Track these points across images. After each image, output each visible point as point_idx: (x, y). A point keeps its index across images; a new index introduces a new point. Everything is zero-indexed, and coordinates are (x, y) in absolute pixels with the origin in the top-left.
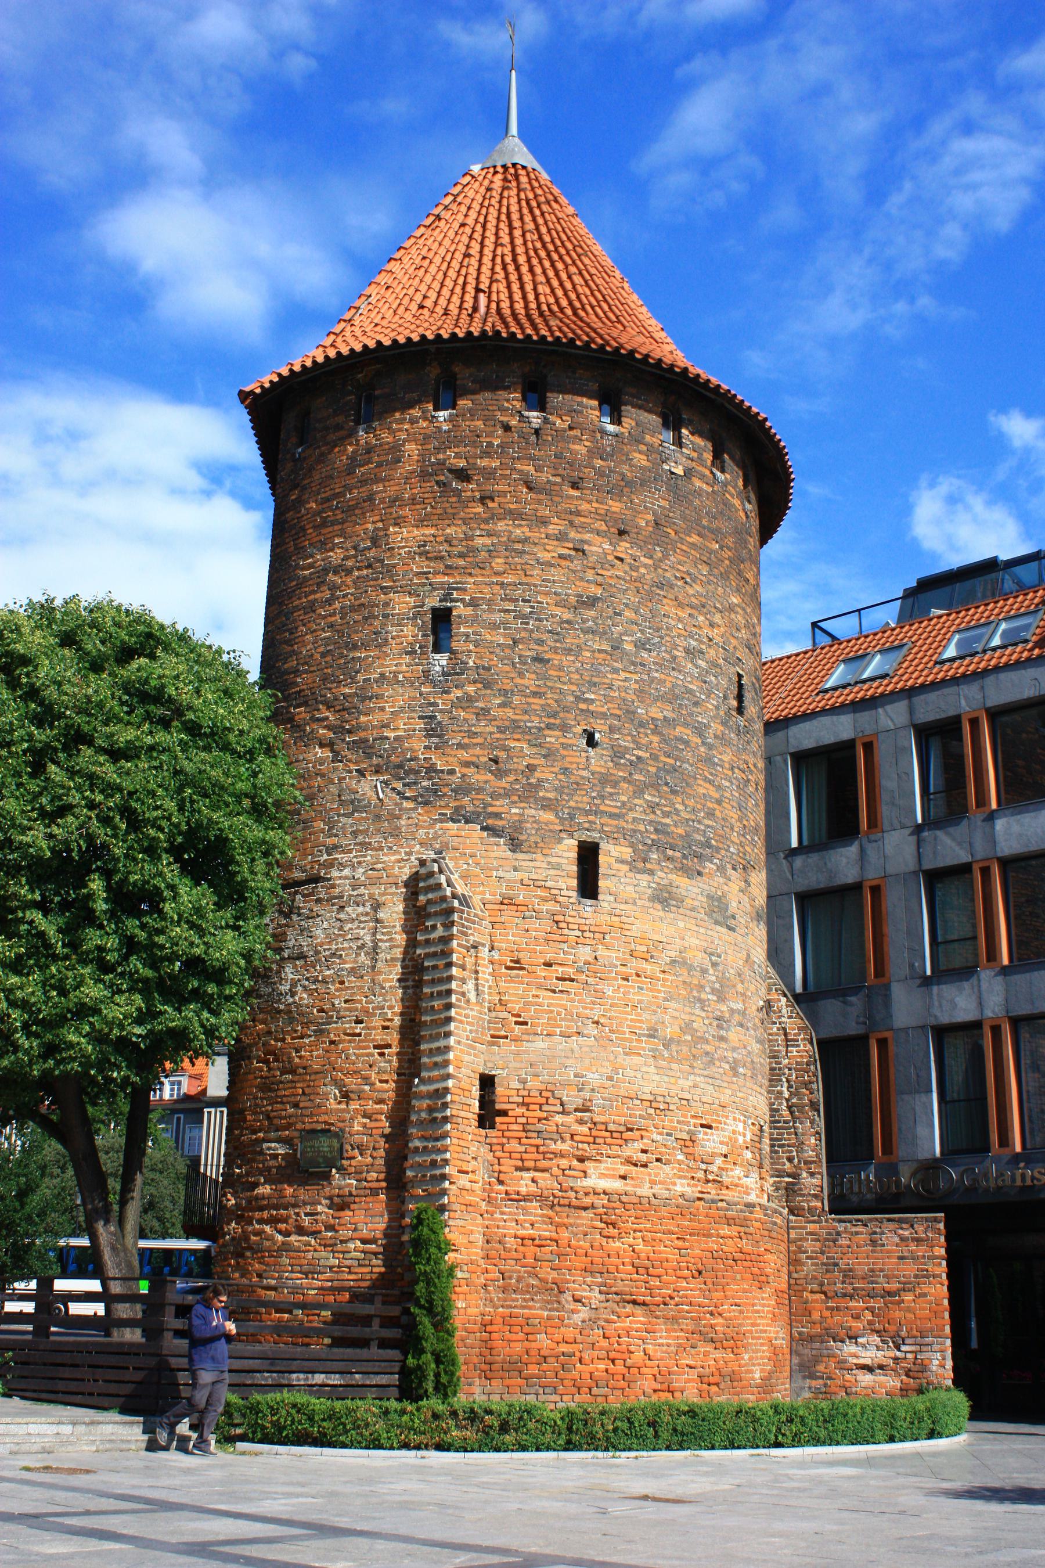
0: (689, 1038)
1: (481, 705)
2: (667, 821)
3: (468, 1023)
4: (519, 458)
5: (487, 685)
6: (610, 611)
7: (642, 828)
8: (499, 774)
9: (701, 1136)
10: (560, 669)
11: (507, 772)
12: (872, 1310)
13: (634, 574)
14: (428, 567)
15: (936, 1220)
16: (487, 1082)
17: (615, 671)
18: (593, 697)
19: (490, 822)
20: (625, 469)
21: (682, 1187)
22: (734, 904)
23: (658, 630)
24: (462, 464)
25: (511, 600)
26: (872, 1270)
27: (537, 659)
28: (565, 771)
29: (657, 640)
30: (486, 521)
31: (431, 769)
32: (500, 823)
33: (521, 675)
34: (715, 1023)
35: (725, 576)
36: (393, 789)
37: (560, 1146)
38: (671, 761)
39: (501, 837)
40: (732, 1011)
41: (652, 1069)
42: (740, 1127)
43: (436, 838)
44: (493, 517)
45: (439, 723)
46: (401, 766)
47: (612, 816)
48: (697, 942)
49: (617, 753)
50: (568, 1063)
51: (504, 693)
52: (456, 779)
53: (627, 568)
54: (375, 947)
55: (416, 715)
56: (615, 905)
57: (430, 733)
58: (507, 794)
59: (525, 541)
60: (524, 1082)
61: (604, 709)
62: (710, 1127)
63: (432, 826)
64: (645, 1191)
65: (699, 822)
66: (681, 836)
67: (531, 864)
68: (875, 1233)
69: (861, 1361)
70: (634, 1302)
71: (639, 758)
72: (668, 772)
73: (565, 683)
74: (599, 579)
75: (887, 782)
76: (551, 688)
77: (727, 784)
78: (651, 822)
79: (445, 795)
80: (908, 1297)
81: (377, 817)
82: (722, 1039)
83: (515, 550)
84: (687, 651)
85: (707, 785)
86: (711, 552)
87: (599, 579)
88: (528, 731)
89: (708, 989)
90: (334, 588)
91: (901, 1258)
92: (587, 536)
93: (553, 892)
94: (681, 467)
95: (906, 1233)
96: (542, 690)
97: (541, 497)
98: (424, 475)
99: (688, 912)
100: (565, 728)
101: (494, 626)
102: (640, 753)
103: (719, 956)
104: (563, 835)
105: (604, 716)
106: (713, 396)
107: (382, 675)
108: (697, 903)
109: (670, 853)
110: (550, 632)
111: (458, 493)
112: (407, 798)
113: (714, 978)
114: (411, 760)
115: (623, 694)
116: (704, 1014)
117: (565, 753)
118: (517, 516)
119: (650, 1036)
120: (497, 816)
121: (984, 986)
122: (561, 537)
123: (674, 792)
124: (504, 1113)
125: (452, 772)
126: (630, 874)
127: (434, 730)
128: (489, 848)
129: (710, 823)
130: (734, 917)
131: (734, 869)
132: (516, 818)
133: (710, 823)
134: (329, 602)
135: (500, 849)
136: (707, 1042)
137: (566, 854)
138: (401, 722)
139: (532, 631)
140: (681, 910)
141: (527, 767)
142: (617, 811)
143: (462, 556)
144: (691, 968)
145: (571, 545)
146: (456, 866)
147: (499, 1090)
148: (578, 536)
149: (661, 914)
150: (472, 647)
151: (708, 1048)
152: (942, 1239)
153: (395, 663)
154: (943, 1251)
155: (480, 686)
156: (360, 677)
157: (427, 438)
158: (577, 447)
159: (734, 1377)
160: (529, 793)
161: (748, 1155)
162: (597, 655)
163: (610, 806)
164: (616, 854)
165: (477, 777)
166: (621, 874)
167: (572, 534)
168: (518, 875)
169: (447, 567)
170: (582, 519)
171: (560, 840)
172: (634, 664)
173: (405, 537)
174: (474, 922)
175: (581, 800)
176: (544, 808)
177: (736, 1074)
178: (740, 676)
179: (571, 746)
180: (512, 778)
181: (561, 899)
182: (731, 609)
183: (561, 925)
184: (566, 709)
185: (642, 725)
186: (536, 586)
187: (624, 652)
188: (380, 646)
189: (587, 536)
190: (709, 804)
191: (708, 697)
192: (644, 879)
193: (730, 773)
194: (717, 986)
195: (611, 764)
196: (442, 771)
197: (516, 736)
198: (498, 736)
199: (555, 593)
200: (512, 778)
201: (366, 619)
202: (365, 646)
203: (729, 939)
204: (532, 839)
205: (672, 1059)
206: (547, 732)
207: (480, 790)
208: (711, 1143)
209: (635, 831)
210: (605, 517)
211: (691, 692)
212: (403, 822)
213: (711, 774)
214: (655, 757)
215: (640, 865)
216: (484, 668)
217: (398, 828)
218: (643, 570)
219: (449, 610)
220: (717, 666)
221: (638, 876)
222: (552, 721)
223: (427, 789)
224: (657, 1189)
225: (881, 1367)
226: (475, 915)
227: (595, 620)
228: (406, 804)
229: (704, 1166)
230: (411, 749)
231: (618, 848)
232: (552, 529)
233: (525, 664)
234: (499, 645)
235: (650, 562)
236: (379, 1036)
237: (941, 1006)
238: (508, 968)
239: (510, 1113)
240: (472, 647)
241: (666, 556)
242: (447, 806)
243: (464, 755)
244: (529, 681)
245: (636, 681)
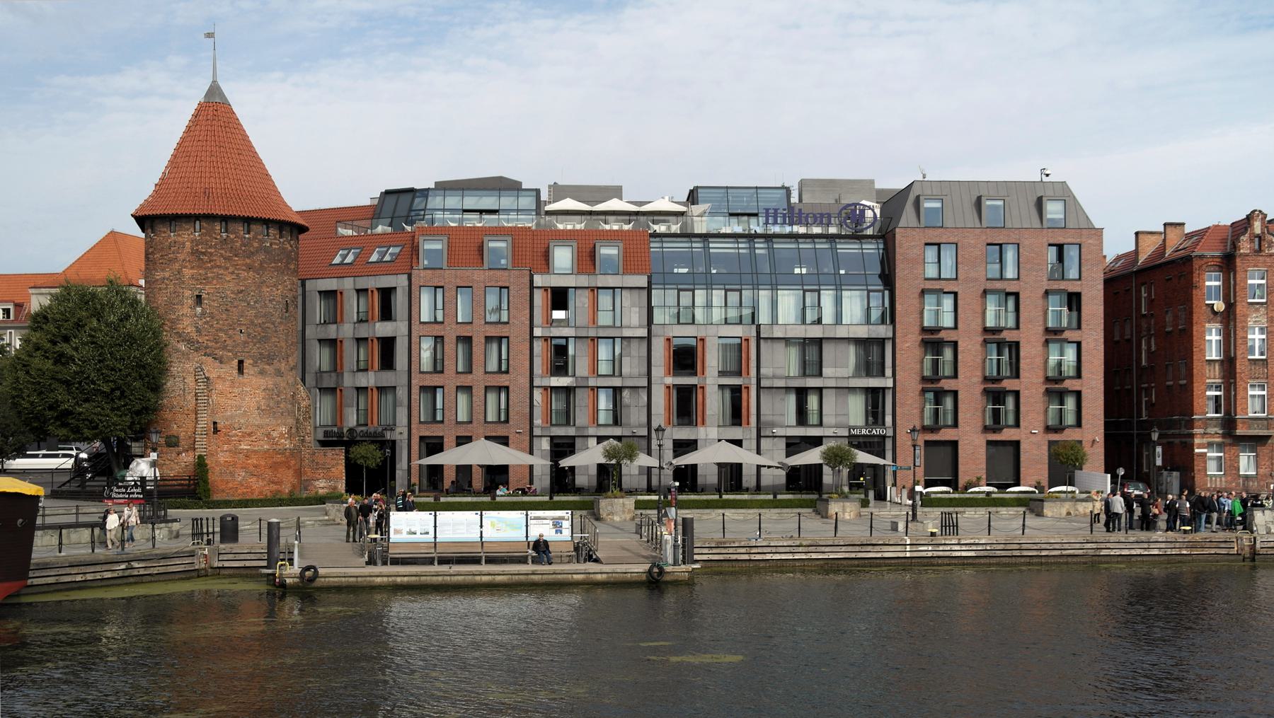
16: (215, 423)
44: (212, 267)
49: (249, 335)
75: (346, 307)
118: (219, 267)
122: (233, 273)
127: (198, 331)
135: (217, 363)
153: (186, 310)
160: (224, 348)
173: (187, 272)
208: (275, 434)
210: (246, 265)
244: (224, 316)
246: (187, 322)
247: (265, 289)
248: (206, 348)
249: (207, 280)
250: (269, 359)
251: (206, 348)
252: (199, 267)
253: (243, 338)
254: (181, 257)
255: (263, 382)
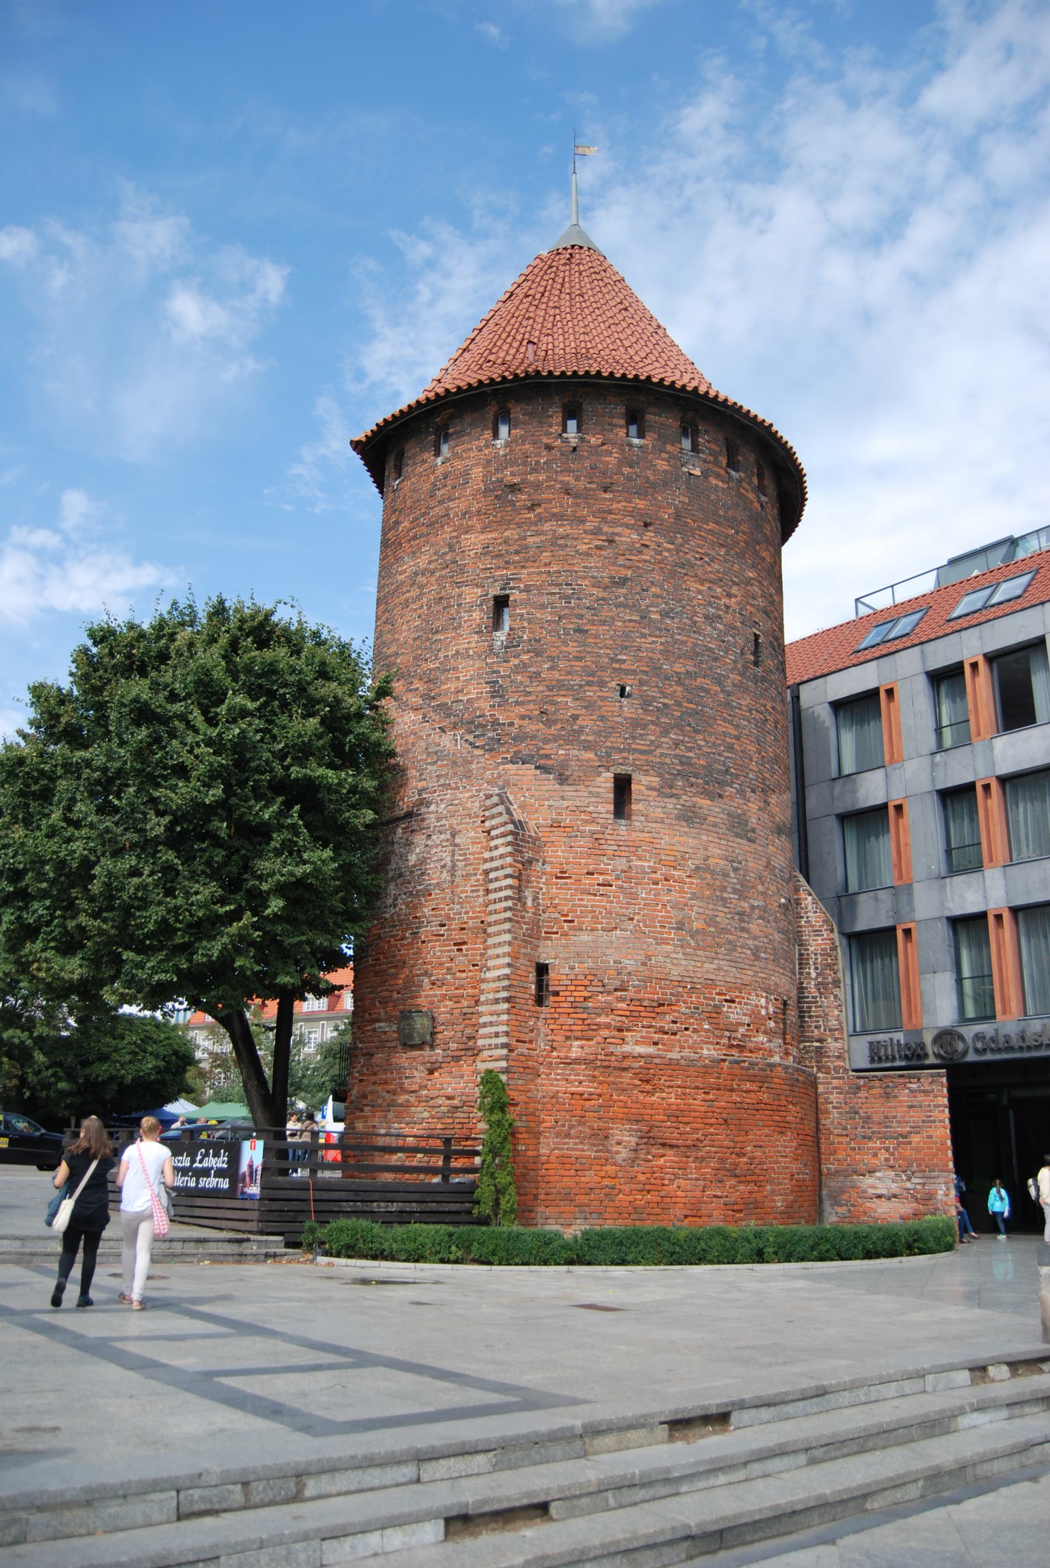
0: (713, 930)
1: (533, 669)
2: (691, 754)
3: (525, 923)
4: (561, 472)
5: (537, 655)
6: (638, 588)
7: (668, 761)
8: (549, 723)
9: (725, 1009)
10: (597, 637)
11: (555, 722)
12: (887, 1149)
13: (659, 557)
14: (491, 563)
15: (939, 1075)
17: (644, 636)
18: (624, 657)
19: (542, 762)
20: (649, 473)
21: (709, 1052)
22: (754, 821)
23: (680, 601)
24: (516, 480)
25: (557, 585)
26: (886, 1117)
27: (578, 630)
28: (602, 718)
29: (679, 609)
30: (536, 524)
31: (496, 723)
32: (550, 762)
33: (565, 643)
34: (737, 917)
35: (741, 555)
36: (466, 740)
37: (603, 1019)
38: (694, 707)
39: (550, 773)
40: (753, 907)
41: (680, 956)
42: (763, 1001)
43: (499, 777)
44: (540, 519)
45: (501, 686)
46: (472, 722)
47: (642, 752)
48: (719, 852)
49: (646, 702)
50: (608, 952)
51: (551, 659)
52: (514, 730)
53: (653, 553)
54: (454, 866)
55: (482, 681)
56: (645, 824)
57: (494, 694)
58: (555, 739)
59: (566, 537)
60: (572, 968)
61: (634, 668)
62: (733, 1002)
63: (495, 768)
64: (674, 1055)
65: (720, 755)
66: (703, 766)
67: (575, 794)
68: (888, 1086)
69: (879, 1192)
70: (663, 1145)
71: (664, 705)
72: (690, 715)
73: (601, 648)
74: (628, 563)
76: (589, 652)
77: (746, 723)
78: (675, 756)
79: (506, 743)
80: (915, 1139)
81: (454, 763)
82: (743, 930)
83: (559, 545)
84: (706, 617)
85: (726, 725)
86: (727, 536)
87: (628, 563)
88: (570, 688)
89: (729, 890)
90: (421, 587)
91: (911, 1107)
92: (618, 530)
93: (594, 815)
94: (698, 469)
95: (914, 1086)
96: (583, 655)
97: (579, 501)
98: (487, 490)
99: (710, 828)
100: (602, 684)
101: (543, 607)
102: (666, 701)
103: (740, 863)
104: (601, 769)
105: (634, 672)
106: (722, 409)
107: (458, 652)
108: (718, 820)
109: (693, 780)
110: (588, 608)
111: (512, 503)
112: (477, 747)
113: (735, 881)
114: (480, 716)
115: (650, 654)
116: (726, 910)
117: (602, 704)
119: (677, 929)
120: (547, 757)
121: (988, 882)
122: (596, 532)
123: (697, 731)
124: (557, 994)
125: (511, 724)
126: (659, 799)
127: (497, 692)
128: (542, 783)
129: (729, 755)
130: (753, 831)
131: (753, 791)
132: (562, 758)
133: (729, 755)
134: (419, 598)
135: (550, 783)
136: (728, 932)
137: (603, 785)
138: (471, 687)
139: (573, 608)
140: (704, 827)
141: (571, 716)
142: (645, 748)
143: (517, 552)
144: (713, 873)
145: (604, 538)
146: (516, 798)
147: (552, 974)
148: (610, 530)
149: (686, 829)
150: (526, 624)
151: (731, 937)
152: (945, 1090)
154: (946, 1101)
155: (532, 654)
156: (441, 655)
157: (489, 462)
158: (608, 459)
159: (757, 1205)
160: (573, 737)
161: (772, 1024)
162: (627, 624)
163: (640, 744)
164: (647, 783)
165: (531, 726)
166: (651, 799)
167: (605, 529)
168: (565, 803)
169: (507, 562)
170: (613, 516)
171: (599, 774)
172: (660, 630)
174: (528, 842)
175: (615, 741)
176: (586, 749)
177: (757, 958)
178: (757, 637)
179: (606, 698)
180: (559, 726)
181: (601, 821)
182: (748, 582)
183: (601, 842)
184: (603, 669)
185: (667, 678)
186: (576, 572)
187: (651, 620)
188: (455, 629)
189: (618, 530)
190: (728, 740)
191: (726, 653)
192: (670, 803)
193: (748, 714)
194: (739, 887)
195: (641, 711)
196: (504, 724)
197: (562, 693)
198: (547, 693)
199: (592, 577)
200: (559, 726)
201: (444, 608)
202: (444, 630)
203: (747, 848)
204: (576, 774)
205: (698, 947)
206: (587, 688)
207: (533, 737)
209: (662, 764)
211: (710, 650)
212: (474, 766)
213: (730, 715)
214: (679, 704)
215: (667, 791)
216: (535, 640)
217: (470, 771)
218: (666, 554)
219: (507, 596)
220: (735, 628)
221: (666, 800)
222: (591, 679)
223: (492, 739)
224: (686, 1053)
225: (895, 1196)
226: (530, 837)
227: (625, 596)
228: (478, 752)
229: (727, 1034)
230: (479, 708)
231: (648, 778)
232: (589, 526)
233: (569, 634)
234: (547, 621)
235: (672, 547)
236: (458, 937)
237: (953, 900)
238: (557, 878)
239: (561, 994)
240: (526, 624)
241: (687, 542)
242: (507, 752)
243: (522, 710)
244: (572, 648)
245: (662, 644)
246: (468, 669)
247: (695, 586)
248: (519, 738)
249: (525, 555)
250: (713, 781)
251: (519, 738)
252: (504, 523)
253: (629, 708)
254: (456, 507)
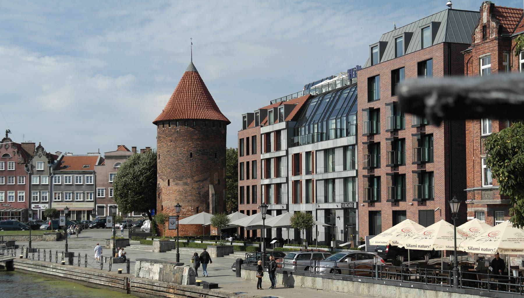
160: (164, 175)
178: (191, 153)
247: (178, 149)
250: (180, 178)
253: (169, 170)
255: (175, 188)
